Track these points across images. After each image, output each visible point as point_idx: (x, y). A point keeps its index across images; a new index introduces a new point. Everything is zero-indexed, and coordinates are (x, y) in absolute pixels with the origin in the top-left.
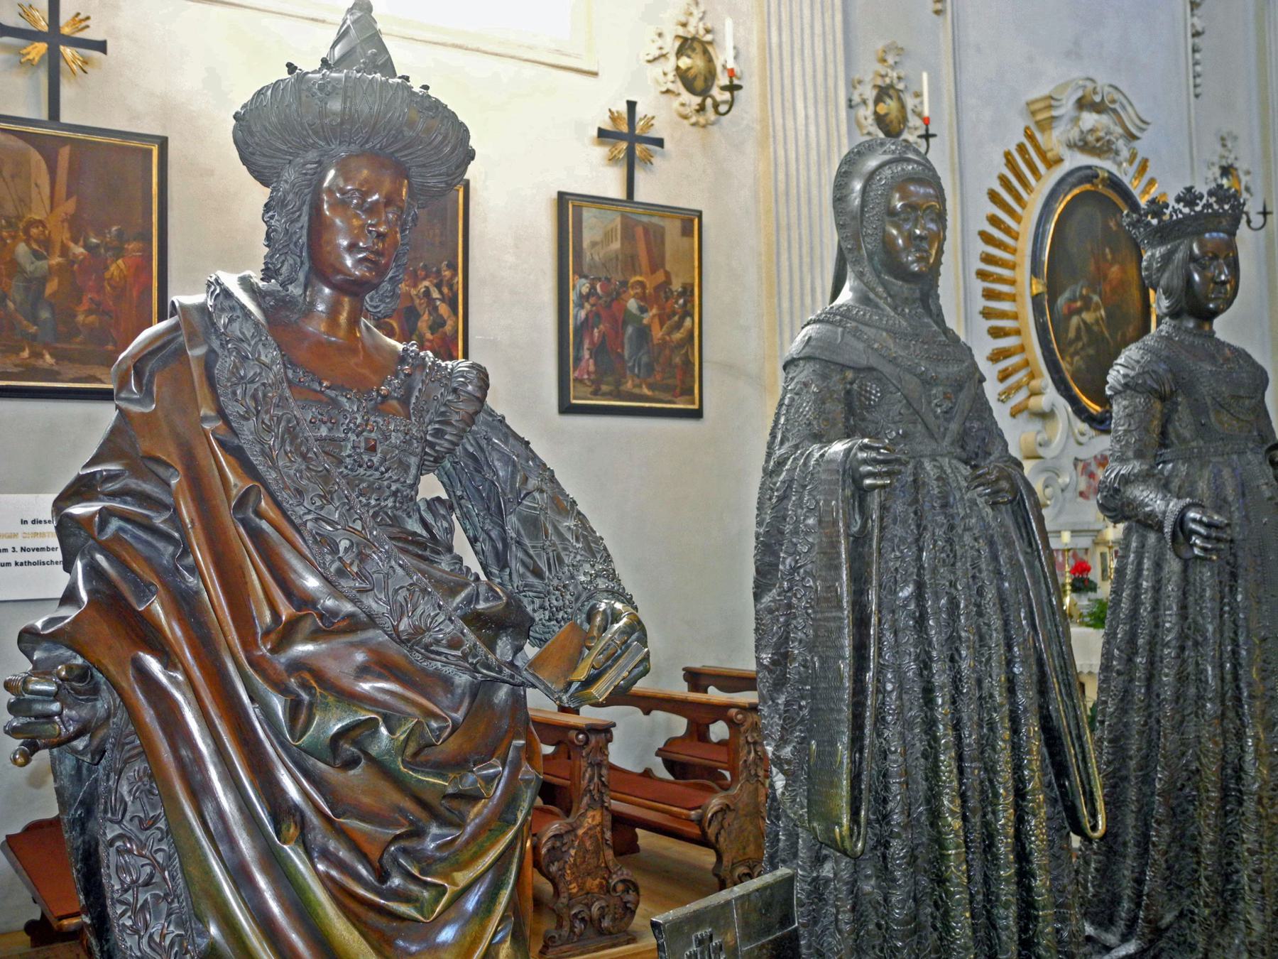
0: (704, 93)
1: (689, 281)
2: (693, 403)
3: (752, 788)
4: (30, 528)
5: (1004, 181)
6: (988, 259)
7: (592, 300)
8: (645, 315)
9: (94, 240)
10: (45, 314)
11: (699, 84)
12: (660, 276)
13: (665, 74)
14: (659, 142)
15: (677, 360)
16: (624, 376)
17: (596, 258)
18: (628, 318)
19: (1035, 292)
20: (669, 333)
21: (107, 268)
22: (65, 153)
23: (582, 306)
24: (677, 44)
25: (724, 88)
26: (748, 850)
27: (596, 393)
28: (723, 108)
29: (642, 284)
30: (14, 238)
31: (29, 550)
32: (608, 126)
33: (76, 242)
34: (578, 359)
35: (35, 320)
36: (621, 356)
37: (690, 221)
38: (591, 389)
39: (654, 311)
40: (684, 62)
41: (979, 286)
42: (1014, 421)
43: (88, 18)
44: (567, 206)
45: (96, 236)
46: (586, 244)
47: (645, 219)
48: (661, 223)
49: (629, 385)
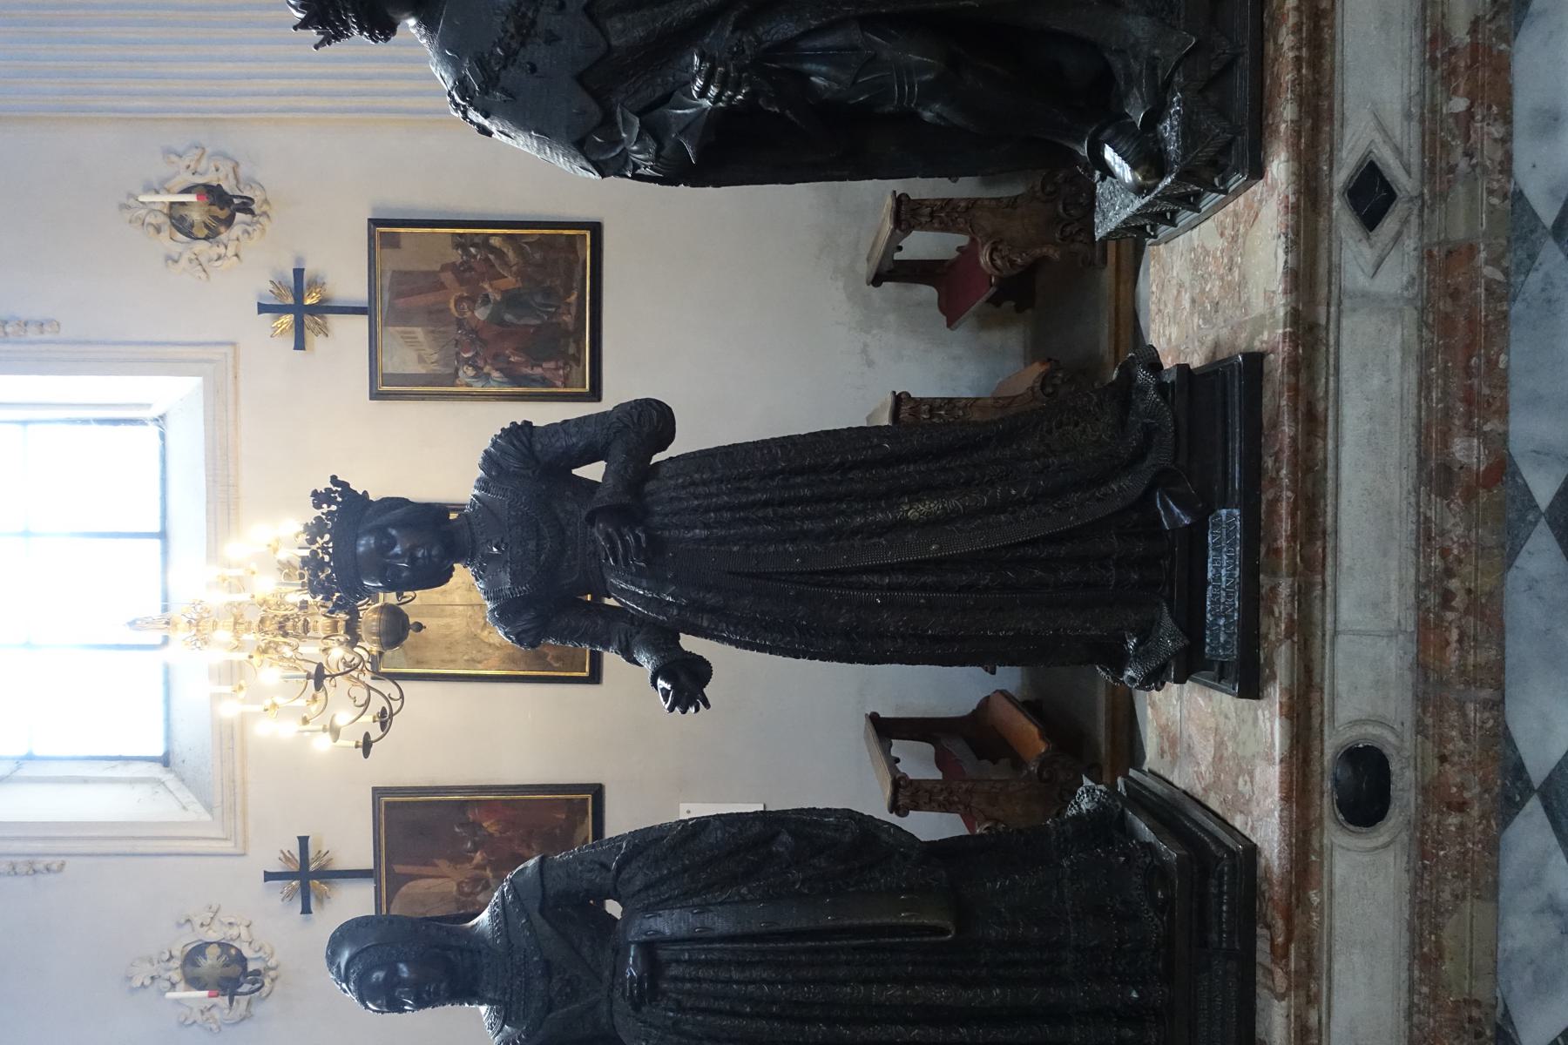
7: (480, 363)
12: (448, 277)
21: (491, 835)
22: (398, 868)
23: (488, 376)
27: (578, 360)
29: (458, 301)
34: (544, 382)
36: (538, 327)
37: (385, 230)
39: (486, 286)
44: (385, 388)
46: (420, 370)
47: (387, 297)
48: (389, 274)
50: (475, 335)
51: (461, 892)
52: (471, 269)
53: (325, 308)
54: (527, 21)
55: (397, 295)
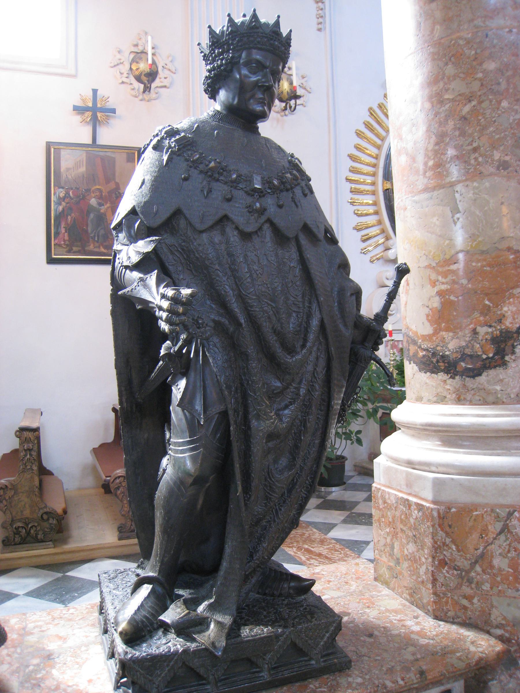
3: (29, 476)
5: (367, 125)
6: (353, 170)
7: (67, 200)
8: (102, 207)
12: (112, 186)
13: (121, 74)
14: (113, 111)
17: (70, 177)
18: (90, 209)
19: (385, 188)
23: (60, 204)
24: (132, 56)
26: (25, 513)
27: (69, 252)
32: (80, 104)
34: (57, 234)
36: (87, 231)
38: (65, 250)
39: (108, 205)
41: (349, 185)
42: (373, 265)
44: (52, 151)
46: (63, 169)
47: (102, 154)
48: (113, 156)
49: (91, 247)
50: (82, 198)
53: (95, 123)
54: (217, 176)
55: (103, 159)
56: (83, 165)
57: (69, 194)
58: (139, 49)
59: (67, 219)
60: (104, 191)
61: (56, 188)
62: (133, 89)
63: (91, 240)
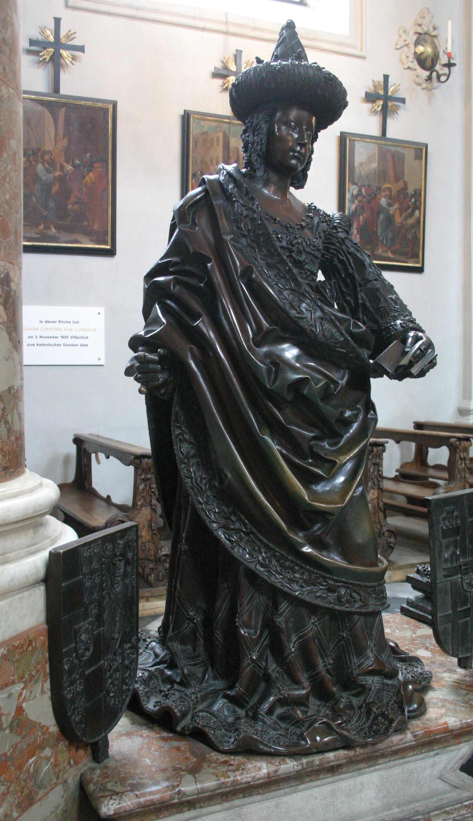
0: (431, 68)
1: (418, 187)
2: (418, 263)
4: (44, 325)
7: (360, 198)
9: (77, 162)
10: (52, 204)
11: (429, 63)
12: (401, 185)
14: (403, 101)
15: (410, 236)
16: (377, 246)
17: (363, 173)
18: (380, 210)
20: (405, 220)
21: (84, 177)
23: (353, 202)
24: (415, 37)
25: (445, 65)
28: (443, 78)
29: (390, 189)
30: (36, 161)
31: (44, 337)
33: (67, 162)
35: (46, 208)
36: (376, 233)
37: (421, 151)
39: (397, 206)
40: (420, 49)
43: (75, 33)
45: (79, 160)
46: (356, 164)
47: (393, 149)
51: (44, 153)
52: (405, 198)
53: (385, 113)
56: (375, 159)
57: (361, 192)
58: (423, 29)
59: (359, 219)
60: (393, 190)
61: (350, 184)
62: (418, 76)
63: (380, 243)
